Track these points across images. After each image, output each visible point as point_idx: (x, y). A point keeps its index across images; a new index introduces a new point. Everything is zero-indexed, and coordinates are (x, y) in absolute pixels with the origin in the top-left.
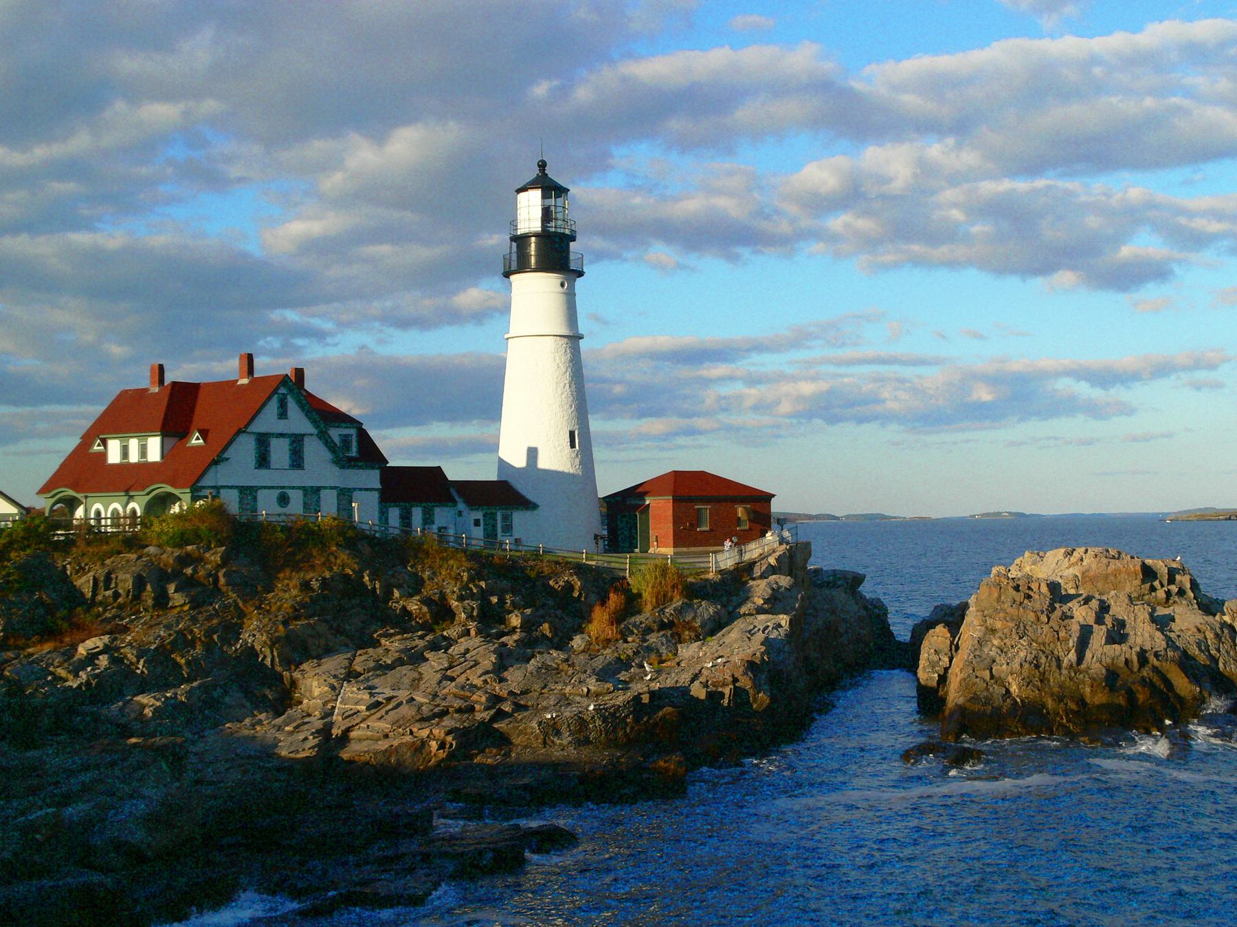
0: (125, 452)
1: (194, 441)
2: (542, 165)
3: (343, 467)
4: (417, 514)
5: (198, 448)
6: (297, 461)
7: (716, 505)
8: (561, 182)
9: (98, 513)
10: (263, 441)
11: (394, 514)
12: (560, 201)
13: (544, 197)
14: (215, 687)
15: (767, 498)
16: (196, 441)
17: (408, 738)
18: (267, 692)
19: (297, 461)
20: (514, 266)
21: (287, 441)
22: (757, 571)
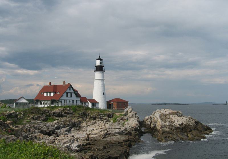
0: (47, 95)
2: (100, 56)
3: (77, 97)
4: (83, 104)
5: (58, 94)
6: (71, 96)
7: (122, 104)
8: (102, 59)
9: (43, 103)
10: (67, 93)
11: (81, 103)
12: (102, 61)
15: (127, 102)
16: (58, 93)
17: (98, 135)
19: (71, 96)
21: (70, 94)
22: (129, 112)
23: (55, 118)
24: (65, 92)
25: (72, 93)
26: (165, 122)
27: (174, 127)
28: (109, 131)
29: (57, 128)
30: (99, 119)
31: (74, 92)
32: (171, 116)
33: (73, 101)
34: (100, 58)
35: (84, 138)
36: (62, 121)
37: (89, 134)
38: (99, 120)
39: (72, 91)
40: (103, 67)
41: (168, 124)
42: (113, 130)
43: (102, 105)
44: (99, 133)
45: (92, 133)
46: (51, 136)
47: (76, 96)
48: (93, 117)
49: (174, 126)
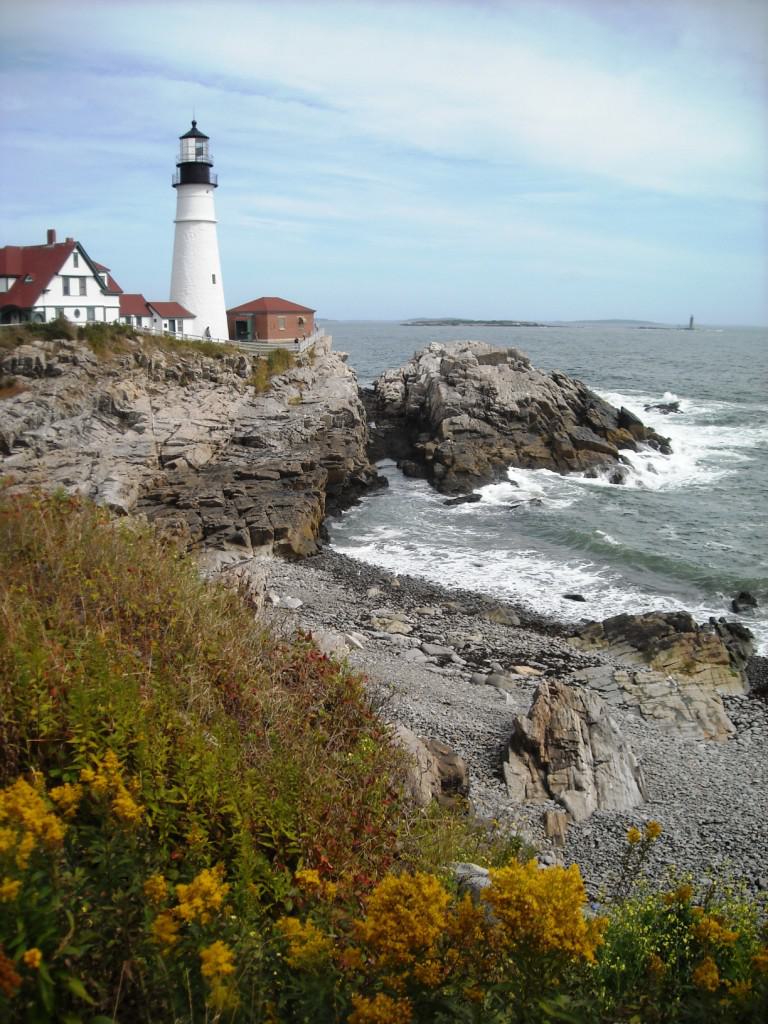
1: (27, 280)
2: (194, 123)
4: (134, 321)
6: (83, 291)
8: (205, 133)
12: (204, 145)
13: (196, 142)
14: (85, 419)
15: (311, 312)
18: (112, 421)
19: (83, 291)
20: (179, 182)
23: (22, 380)
24: (57, 274)
25: (84, 277)
26: (463, 393)
27: (496, 411)
28: (240, 430)
29: (29, 422)
30: (203, 382)
31: (91, 274)
32: (487, 370)
33: (91, 313)
34: (194, 129)
35: (143, 460)
36: (52, 395)
37: (165, 444)
38: (201, 387)
39: (84, 269)
40: (211, 169)
41: (474, 401)
42: (258, 423)
43: (209, 321)
44: (203, 438)
45: (174, 437)
46: (10, 454)
47: (101, 292)
48: (175, 377)
49: (497, 407)
